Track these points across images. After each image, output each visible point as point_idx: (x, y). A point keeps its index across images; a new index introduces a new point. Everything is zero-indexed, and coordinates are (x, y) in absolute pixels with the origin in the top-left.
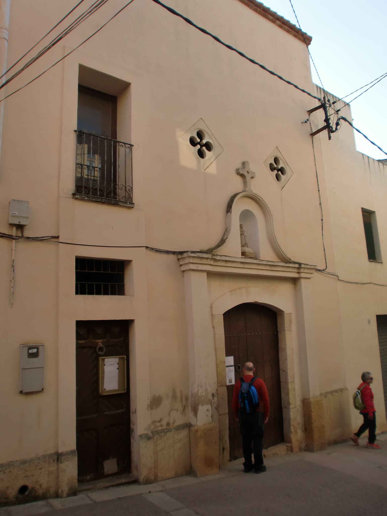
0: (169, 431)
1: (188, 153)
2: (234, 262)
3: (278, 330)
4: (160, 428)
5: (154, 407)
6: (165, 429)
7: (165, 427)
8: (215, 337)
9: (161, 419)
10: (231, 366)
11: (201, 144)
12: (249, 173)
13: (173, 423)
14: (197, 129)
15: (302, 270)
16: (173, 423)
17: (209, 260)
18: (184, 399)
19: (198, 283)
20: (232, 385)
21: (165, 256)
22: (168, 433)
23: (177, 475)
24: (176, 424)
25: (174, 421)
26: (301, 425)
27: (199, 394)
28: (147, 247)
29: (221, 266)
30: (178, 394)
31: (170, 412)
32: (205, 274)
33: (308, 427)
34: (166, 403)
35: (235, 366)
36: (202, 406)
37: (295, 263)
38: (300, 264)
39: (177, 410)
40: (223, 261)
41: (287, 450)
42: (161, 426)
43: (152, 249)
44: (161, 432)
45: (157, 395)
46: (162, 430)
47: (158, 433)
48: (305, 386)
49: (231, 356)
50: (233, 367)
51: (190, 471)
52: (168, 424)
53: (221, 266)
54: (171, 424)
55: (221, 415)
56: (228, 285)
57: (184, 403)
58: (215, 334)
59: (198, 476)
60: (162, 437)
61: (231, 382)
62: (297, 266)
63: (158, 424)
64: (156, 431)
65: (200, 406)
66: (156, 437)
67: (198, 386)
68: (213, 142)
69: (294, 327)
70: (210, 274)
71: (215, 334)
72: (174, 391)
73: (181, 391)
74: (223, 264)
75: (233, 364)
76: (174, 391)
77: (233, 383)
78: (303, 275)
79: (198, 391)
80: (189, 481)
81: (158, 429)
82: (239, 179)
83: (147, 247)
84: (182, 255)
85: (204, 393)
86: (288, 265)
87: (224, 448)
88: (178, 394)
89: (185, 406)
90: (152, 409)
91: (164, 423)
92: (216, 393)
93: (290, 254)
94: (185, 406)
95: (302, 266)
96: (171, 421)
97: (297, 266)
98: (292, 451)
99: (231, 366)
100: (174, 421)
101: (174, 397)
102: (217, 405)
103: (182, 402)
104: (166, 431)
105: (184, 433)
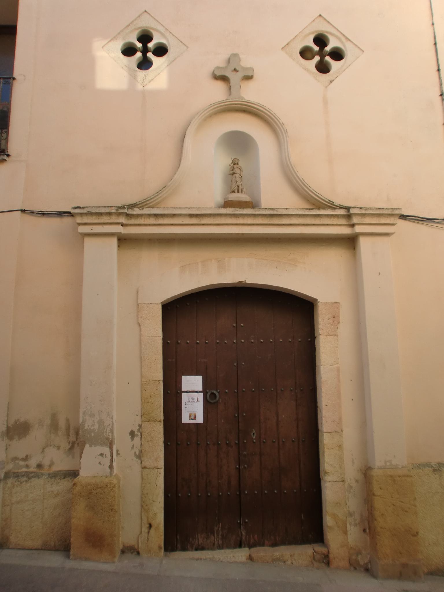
0: (37, 476)
1: (112, 68)
2: (174, 215)
3: (316, 335)
4: (24, 470)
5: (16, 437)
6: (32, 473)
7: (33, 469)
8: (140, 340)
9: (27, 456)
10: (186, 392)
11: (144, 49)
12: (237, 71)
13: (50, 466)
14: (139, 28)
15: (355, 220)
16: (50, 466)
17: (114, 217)
18: (72, 432)
19: (101, 255)
20: (197, 424)
21: (56, 221)
22: (33, 479)
23: (45, 548)
24: (55, 469)
25: (52, 464)
26: (357, 516)
27: (86, 427)
28: (25, 210)
29: (150, 225)
30: (62, 423)
31: (44, 449)
32: (114, 241)
33: (369, 526)
34: (38, 435)
35: (205, 391)
36: (91, 446)
37: (341, 207)
38: (348, 209)
39: (59, 448)
40: (150, 215)
41: (314, 558)
42: (27, 466)
43: (32, 212)
44: (24, 475)
45: (22, 420)
46: (26, 472)
47: (17, 475)
48: (365, 443)
49: (197, 374)
50: (183, 390)
51: (64, 548)
52: (39, 466)
53: (150, 225)
54: (46, 467)
55: (145, 468)
56: (177, 255)
57: (72, 438)
58: (141, 335)
59: (71, 557)
60: (21, 483)
61: (195, 419)
62: (342, 212)
63: (22, 463)
64: (14, 473)
65: (87, 446)
66: (10, 481)
67: (84, 413)
68: (168, 41)
69: (346, 329)
70: (123, 241)
71: (141, 335)
72: (54, 417)
73: (68, 420)
74: (152, 221)
75: (201, 388)
76: (54, 417)
77: (200, 419)
78: (358, 229)
79: (84, 422)
80: (54, 560)
81: (20, 471)
82: (220, 85)
83: (23, 211)
84: (109, 218)
85: (96, 427)
86: (322, 212)
87: (150, 526)
88: (62, 423)
89: (73, 443)
90: (11, 438)
91: (33, 463)
92: (138, 430)
93: (323, 189)
94: (73, 443)
95: (352, 211)
96: (46, 463)
97: (342, 212)
98: (328, 564)
99: (186, 392)
100: (52, 464)
101: (54, 426)
102: (141, 452)
103: (68, 435)
104: (32, 475)
105: (64, 484)
